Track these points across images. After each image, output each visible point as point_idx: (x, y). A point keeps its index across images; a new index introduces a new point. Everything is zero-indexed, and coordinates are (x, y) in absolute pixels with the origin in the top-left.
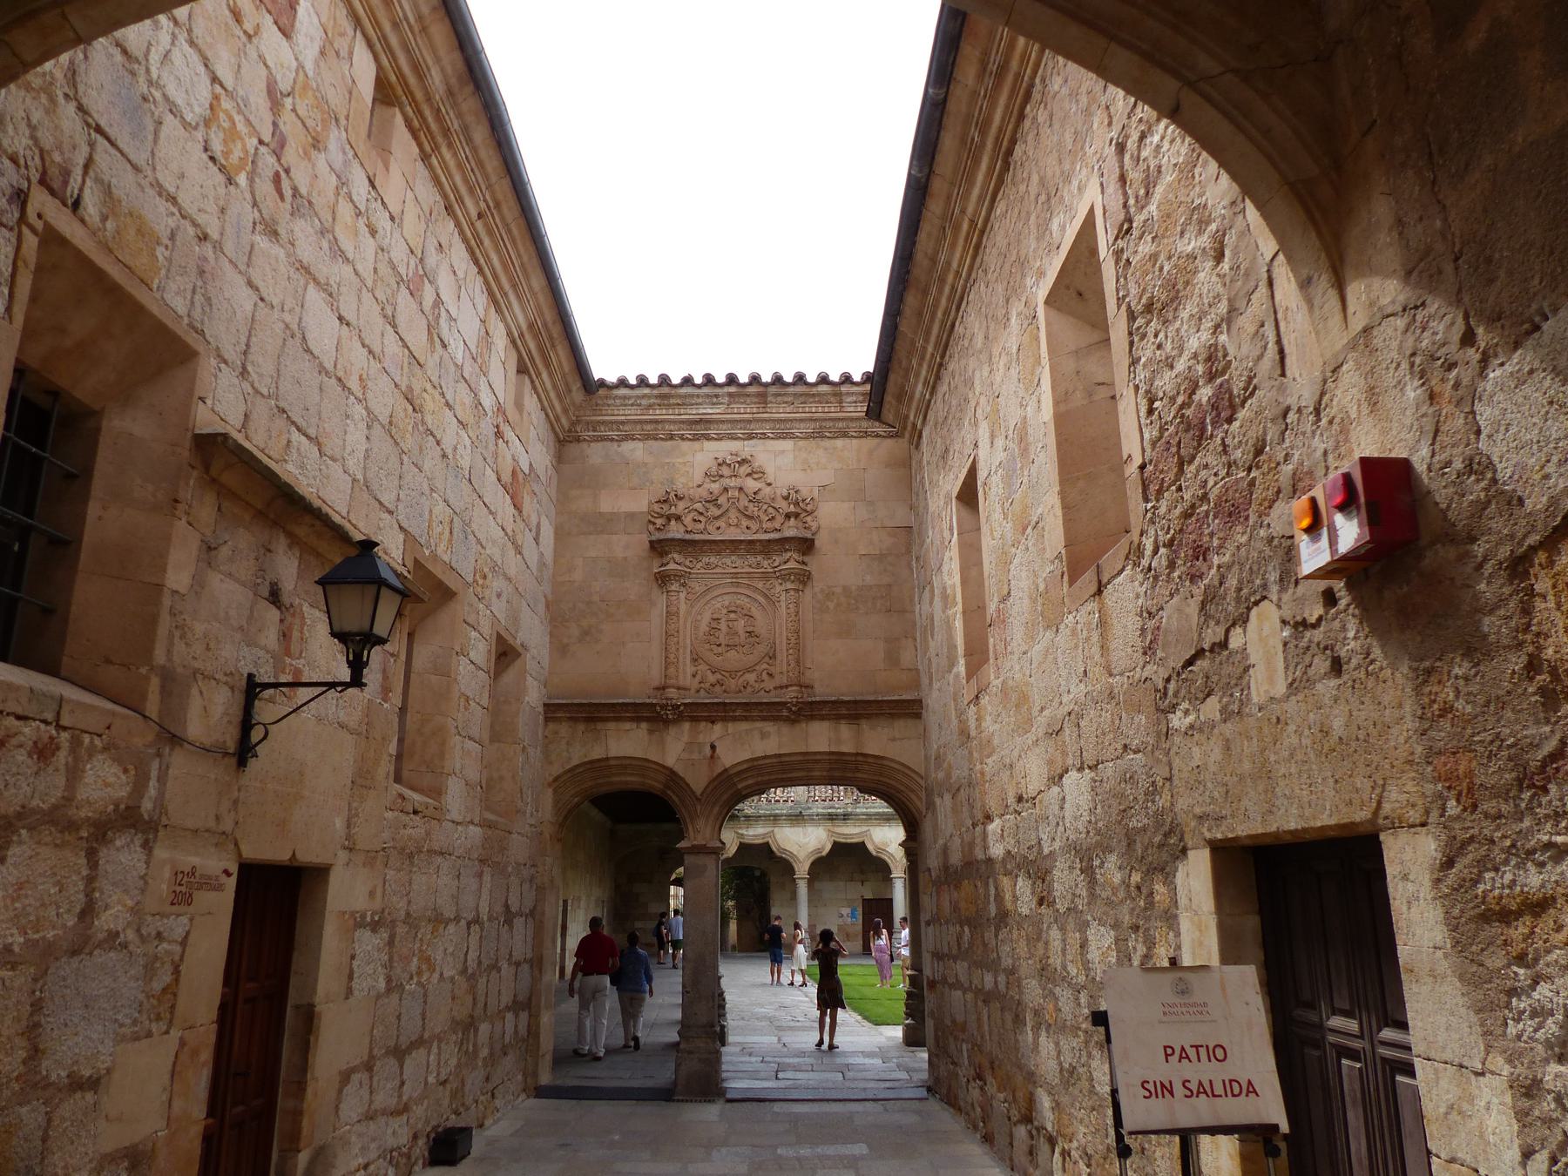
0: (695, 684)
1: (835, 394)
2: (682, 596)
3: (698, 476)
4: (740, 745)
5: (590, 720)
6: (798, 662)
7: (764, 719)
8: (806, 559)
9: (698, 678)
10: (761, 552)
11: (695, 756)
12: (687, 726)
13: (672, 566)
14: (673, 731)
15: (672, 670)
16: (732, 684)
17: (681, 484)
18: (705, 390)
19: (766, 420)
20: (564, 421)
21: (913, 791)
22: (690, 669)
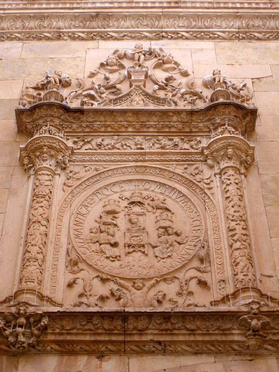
3: (92, 66)
6: (250, 259)
9: (78, 289)
10: (180, 132)
15: (33, 269)
19: (180, 17)
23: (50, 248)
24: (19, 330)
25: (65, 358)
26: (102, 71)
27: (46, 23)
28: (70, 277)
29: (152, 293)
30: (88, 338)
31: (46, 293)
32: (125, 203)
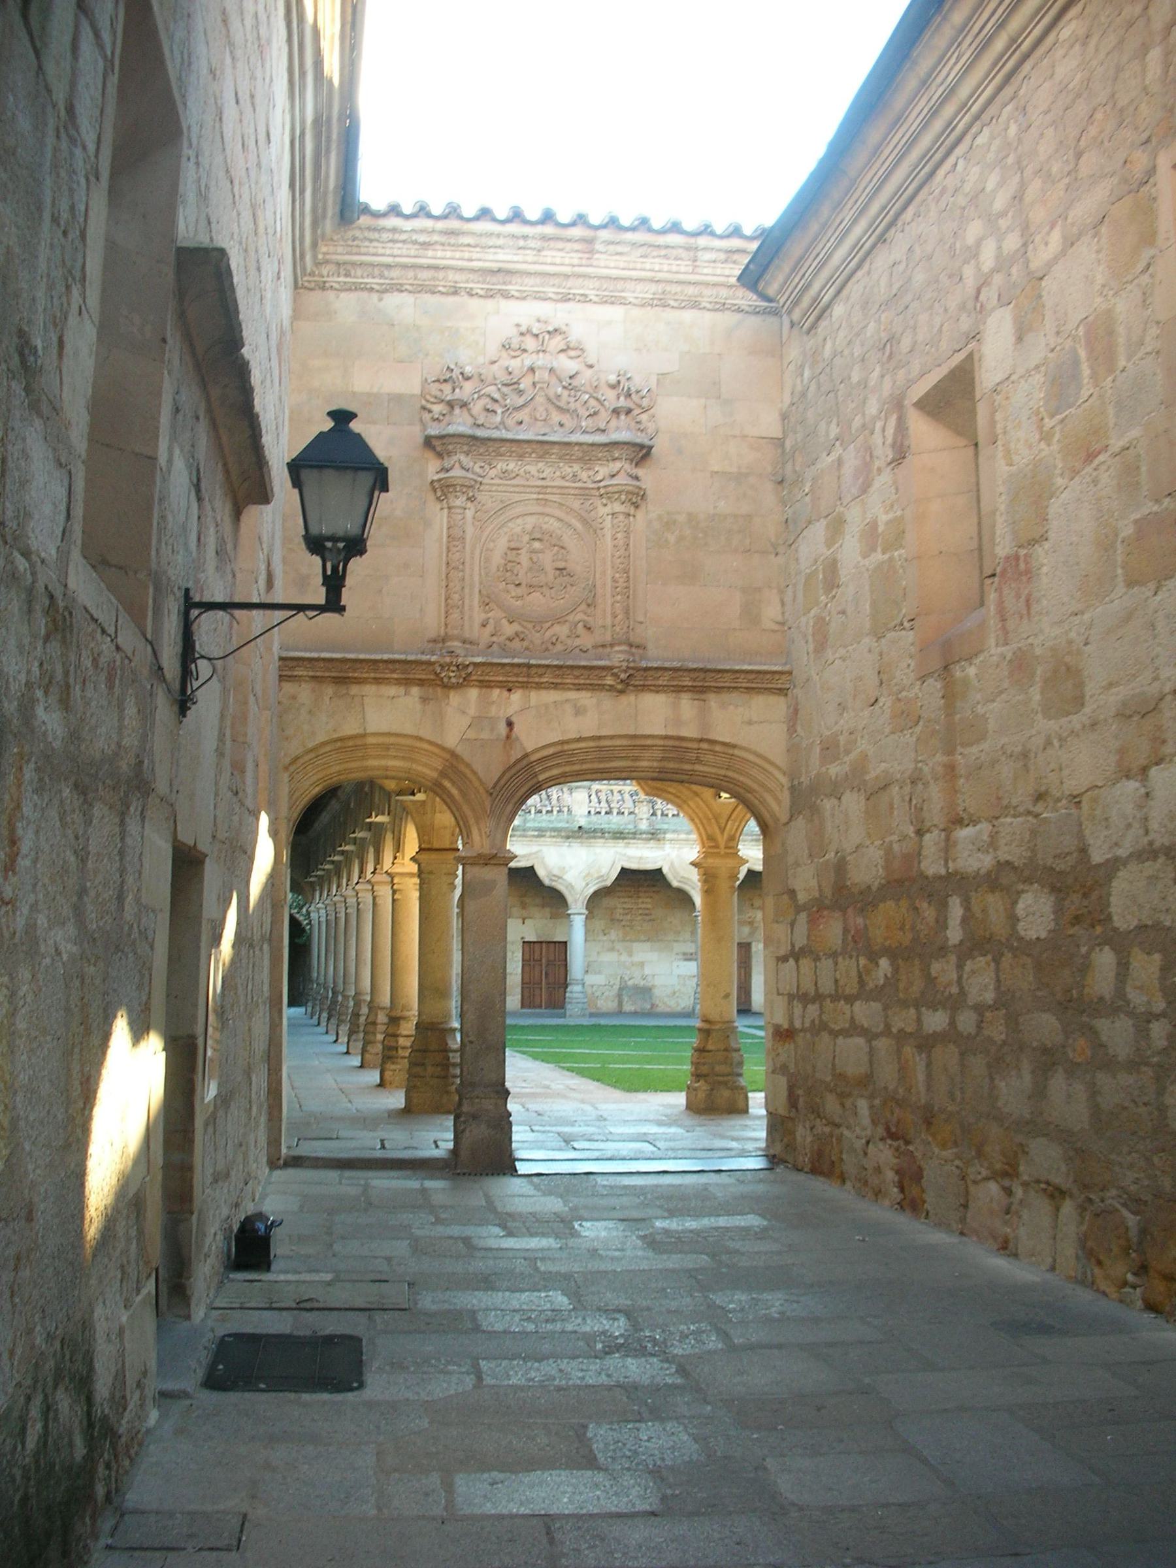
0: (485, 636)
1: (688, 249)
2: (469, 514)
3: (493, 349)
4: (547, 719)
5: (341, 681)
6: (627, 612)
7: (579, 688)
8: (640, 472)
10: (579, 459)
11: (485, 735)
12: (473, 693)
13: (457, 472)
14: (455, 698)
15: (455, 615)
16: (537, 638)
17: (468, 359)
18: (513, 228)
20: (308, 258)
21: (770, 791)
22: (479, 616)
23: (467, 591)
24: (452, 674)
25: (484, 690)
26: (504, 354)
27: (441, 274)
28: (483, 616)
29: (548, 634)
30: (501, 679)
31: (467, 635)
32: (526, 538)
